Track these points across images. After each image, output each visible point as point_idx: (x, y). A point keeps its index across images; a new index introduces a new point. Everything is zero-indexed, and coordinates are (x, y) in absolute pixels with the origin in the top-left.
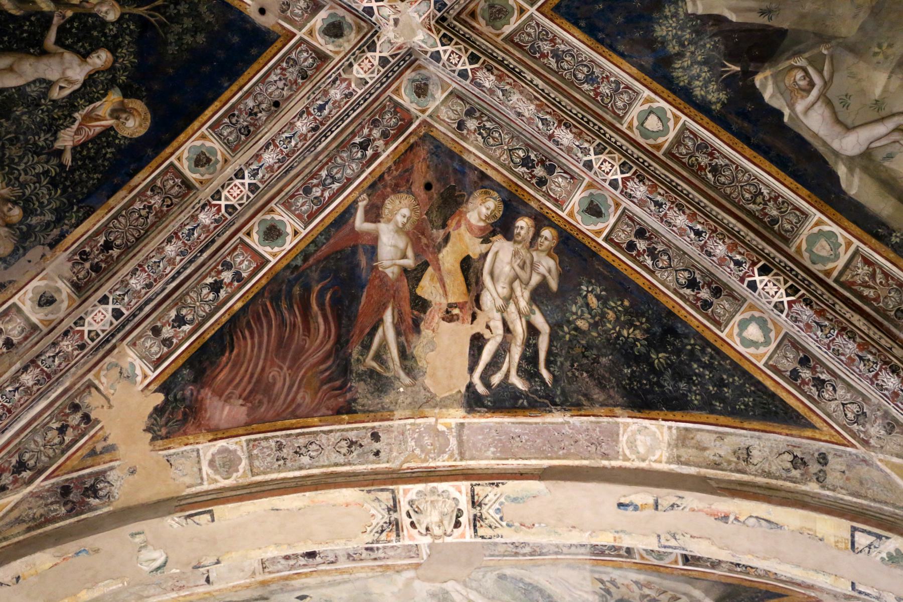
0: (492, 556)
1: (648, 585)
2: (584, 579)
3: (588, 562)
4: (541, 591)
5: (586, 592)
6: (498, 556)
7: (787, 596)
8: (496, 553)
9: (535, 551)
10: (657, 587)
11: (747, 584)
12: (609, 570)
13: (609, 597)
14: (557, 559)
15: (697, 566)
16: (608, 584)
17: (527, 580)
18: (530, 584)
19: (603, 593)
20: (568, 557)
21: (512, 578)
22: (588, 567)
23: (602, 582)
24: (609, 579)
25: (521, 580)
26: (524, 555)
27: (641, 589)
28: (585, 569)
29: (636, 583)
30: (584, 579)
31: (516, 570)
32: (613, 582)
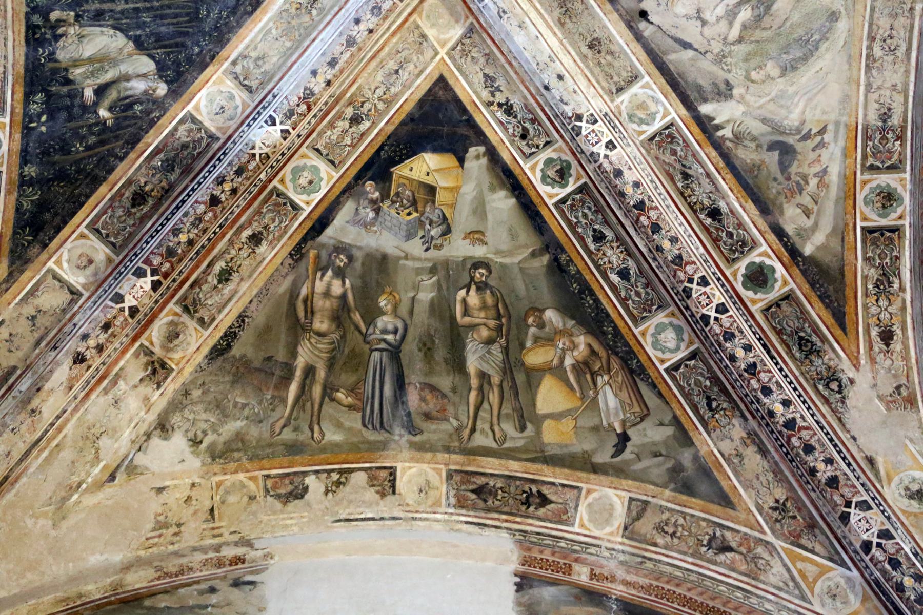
0: (873, 9)
1: (822, 184)
2: (824, 112)
3: (853, 120)
4: (805, 59)
5: (804, 112)
6: (871, 16)
7: (846, 334)
8: (876, 15)
9: (875, 61)
10: (822, 194)
11: (849, 292)
12: (841, 143)
13: (798, 137)
14: (859, 85)
15: (864, 241)
16: (819, 139)
17: (824, 46)
18: (817, 49)
19: (804, 132)
20: (862, 98)
21: (830, 29)
22: (844, 119)
23: (822, 131)
24: (826, 140)
25: (824, 38)
26: (870, 48)
27: (815, 175)
28: (841, 115)
29: (825, 171)
30: (824, 112)
31: (844, 35)
32: (822, 145)
